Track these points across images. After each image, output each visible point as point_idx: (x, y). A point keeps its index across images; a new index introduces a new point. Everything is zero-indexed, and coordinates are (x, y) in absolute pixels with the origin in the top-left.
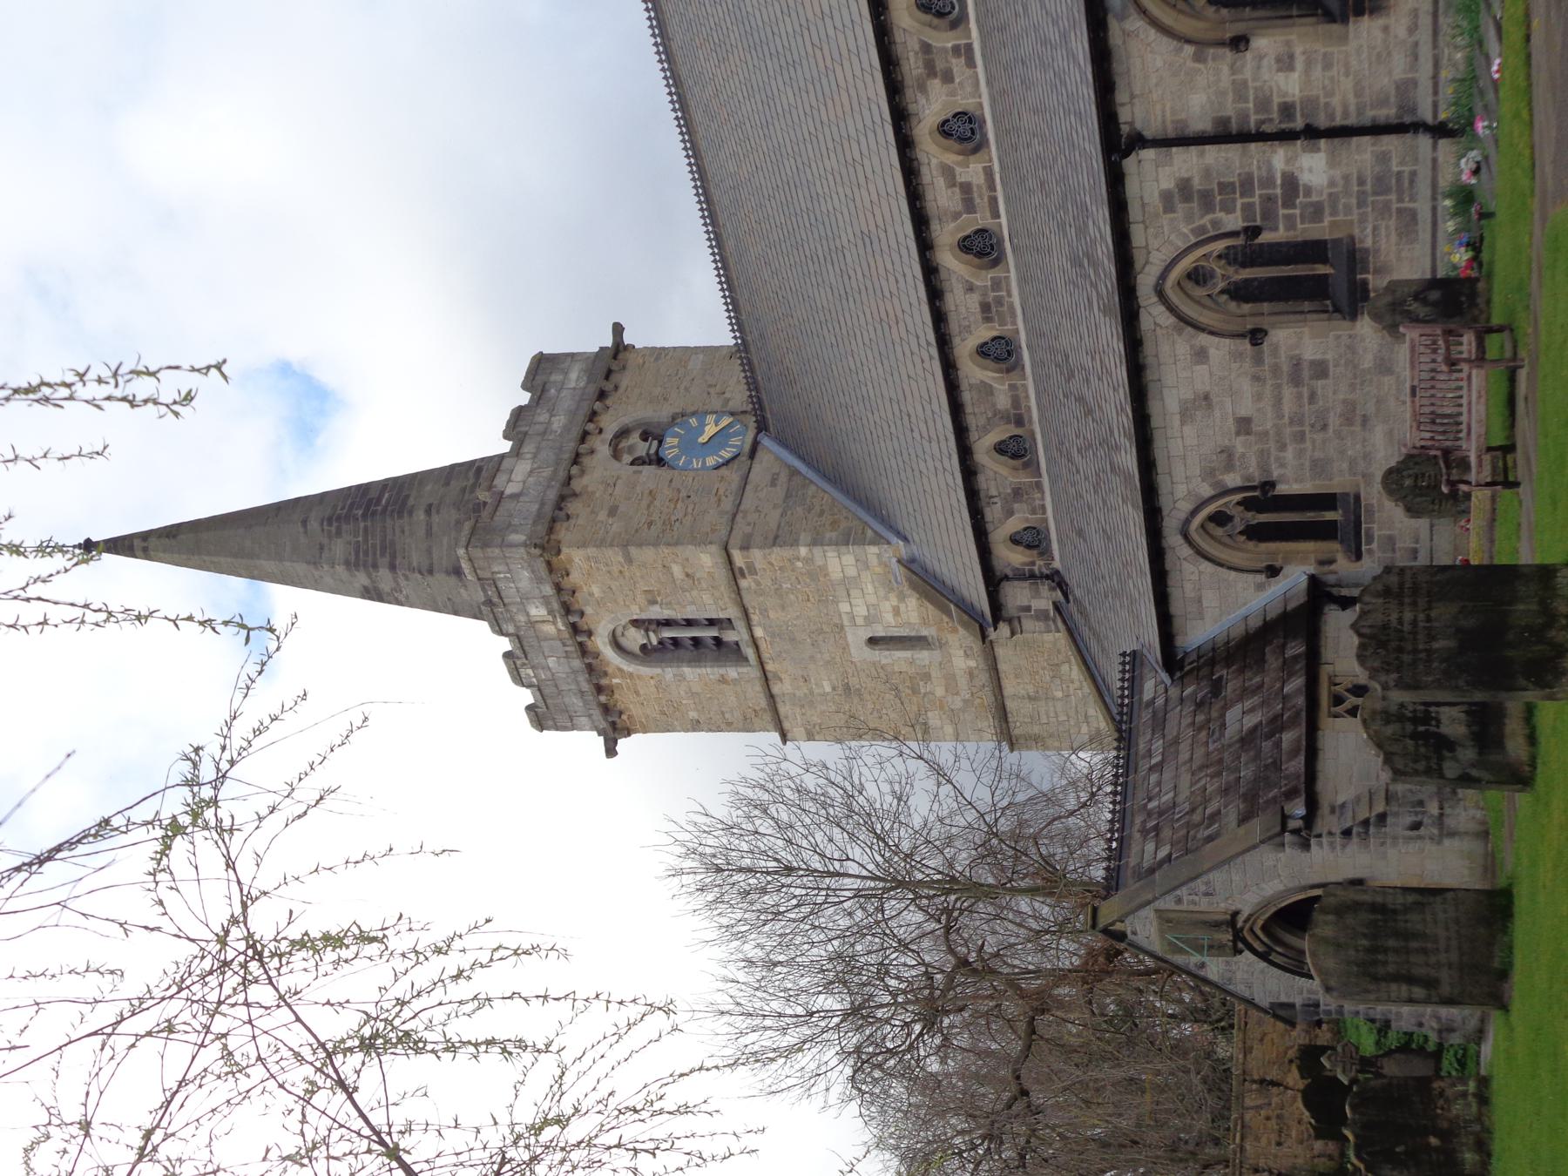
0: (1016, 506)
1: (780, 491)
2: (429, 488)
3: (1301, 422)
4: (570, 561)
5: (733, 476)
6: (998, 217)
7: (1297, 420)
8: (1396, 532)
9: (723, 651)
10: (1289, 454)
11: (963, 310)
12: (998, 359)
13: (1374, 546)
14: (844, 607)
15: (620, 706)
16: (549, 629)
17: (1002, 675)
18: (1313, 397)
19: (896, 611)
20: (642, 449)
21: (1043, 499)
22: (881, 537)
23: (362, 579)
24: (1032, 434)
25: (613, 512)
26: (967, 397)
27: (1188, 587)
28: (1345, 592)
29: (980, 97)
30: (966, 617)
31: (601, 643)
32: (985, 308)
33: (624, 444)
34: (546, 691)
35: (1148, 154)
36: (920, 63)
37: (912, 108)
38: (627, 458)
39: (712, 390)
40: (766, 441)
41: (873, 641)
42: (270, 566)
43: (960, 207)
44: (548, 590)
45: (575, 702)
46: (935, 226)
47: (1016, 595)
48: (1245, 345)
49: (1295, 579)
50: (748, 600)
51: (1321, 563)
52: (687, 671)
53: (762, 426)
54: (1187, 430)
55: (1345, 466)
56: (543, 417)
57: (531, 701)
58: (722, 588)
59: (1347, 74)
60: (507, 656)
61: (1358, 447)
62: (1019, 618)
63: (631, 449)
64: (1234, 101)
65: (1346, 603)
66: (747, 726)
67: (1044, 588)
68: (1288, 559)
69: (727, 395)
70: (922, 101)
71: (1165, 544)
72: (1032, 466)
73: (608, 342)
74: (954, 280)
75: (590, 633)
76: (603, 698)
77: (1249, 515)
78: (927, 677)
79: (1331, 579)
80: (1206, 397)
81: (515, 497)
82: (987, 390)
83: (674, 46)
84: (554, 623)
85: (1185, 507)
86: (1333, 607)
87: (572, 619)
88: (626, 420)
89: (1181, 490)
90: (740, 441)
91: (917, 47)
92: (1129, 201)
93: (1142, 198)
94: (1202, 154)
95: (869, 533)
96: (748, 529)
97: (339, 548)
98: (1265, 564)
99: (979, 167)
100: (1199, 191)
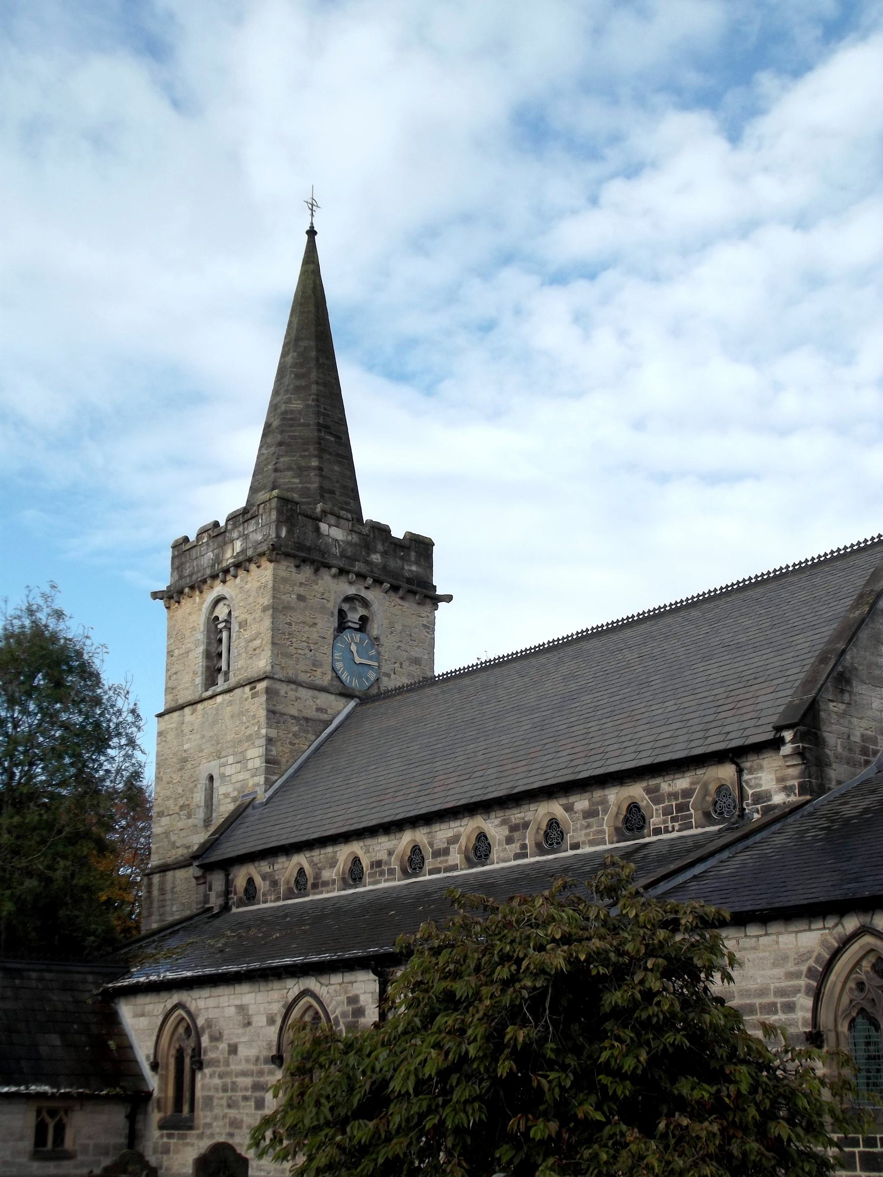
0: (267, 883)
1: (311, 713)
2: (336, 468)
3: (233, 1090)
4: (266, 569)
5: (326, 679)
6: (431, 872)
7: (234, 1087)
8: (171, 1155)
9: (212, 673)
10: (217, 1081)
11: (378, 848)
12: (351, 871)
13: (165, 1140)
14: (231, 760)
15: (183, 602)
16: (229, 554)
17: (187, 869)
18: (245, 1098)
19: (226, 795)
20: (353, 617)
21: (271, 901)
22: (271, 786)
23: (276, 423)
24: (308, 895)
25: (301, 598)
26: (329, 850)
27: (149, 1008)
28: (140, 1117)
29: (497, 863)
30: (207, 845)
31: (219, 589)
32: (379, 864)
33: (357, 603)
34: (194, 551)
36: (517, 822)
37: (493, 815)
38: (346, 607)
39: (397, 665)
40: (352, 704)
41: (211, 778)
42: (289, 359)
43: (436, 847)
44: (250, 553)
45: (187, 572)
47: (217, 881)
48: (274, 1052)
49: (153, 1082)
50: (237, 691)
51: (159, 1101)
52: (201, 648)
53: (365, 699)
54: (233, 1009)
55: (208, 1120)
56: (380, 547)
57: (191, 540)
58: (246, 674)
60: (216, 524)
61: (218, 1130)
62: (205, 883)
63: (354, 609)
65: (132, 1118)
66: (169, 690)
67: (221, 901)
68: (164, 1080)
69: (393, 676)
70: (497, 821)
71: (174, 991)
72: (289, 895)
73: (439, 592)
74: (394, 842)
75: (224, 582)
76: (187, 590)
77: (189, 1051)
78: (189, 816)
79: (150, 1109)
80: (249, 1024)
81: (317, 529)
82: (333, 864)
83: (583, 643)
84: (232, 557)
85: (192, 1007)
86: (129, 1109)
87: (232, 569)
88: (375, 607)
89: (201, 1004)
90: (355, 684)
91: (526, 819)
92: (354, 973)
93: (356, 982)
95: (275, 778)
96: (282, 692)
97: (297, 405)
98: (159, 1060)
99: (458, 862)
100: (357, 1022)
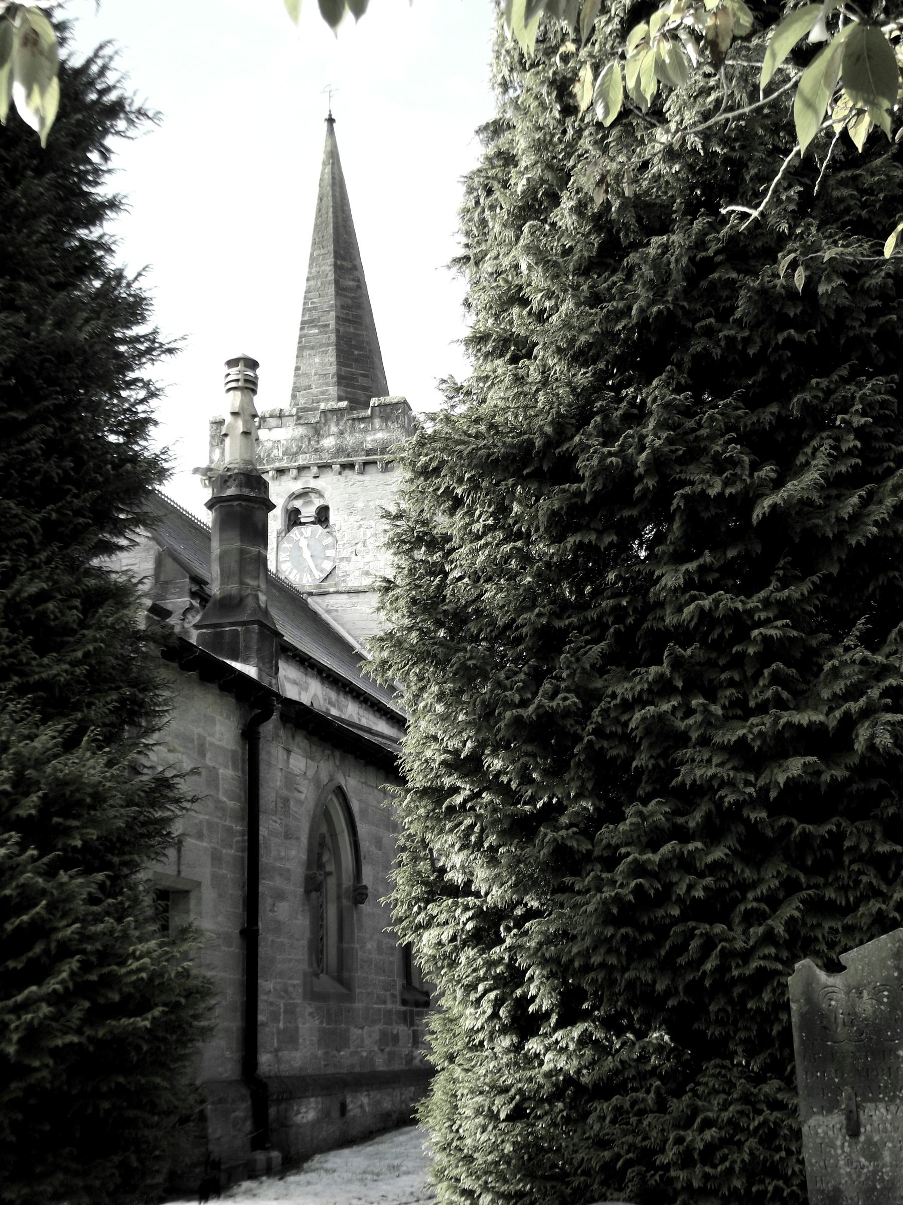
20: (308, 512)
33: (312, 495)
38: (298, 504)
56: (334, 429)
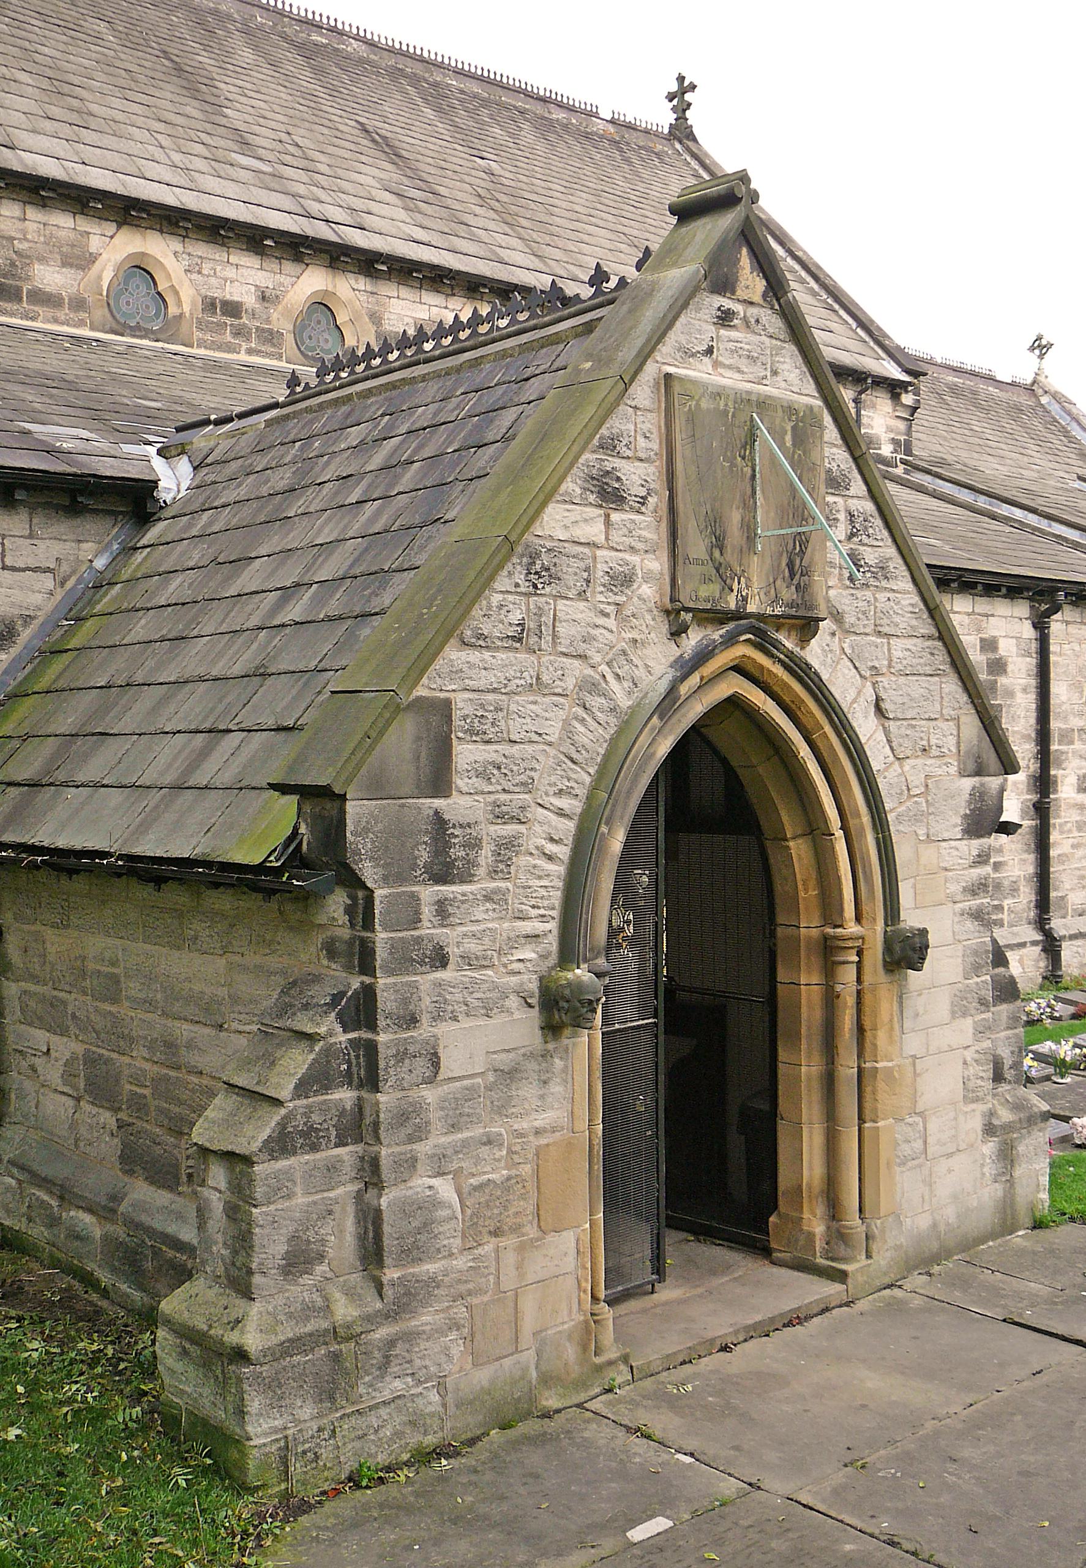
11: (230, 273)
32: (232, 309)
35: (1028, 632)
46: (362, 283)
59: (1073, 846)
64: (1060, 729)
93: (993, 615)
94: (1025, 690)
100: (996, 682)
